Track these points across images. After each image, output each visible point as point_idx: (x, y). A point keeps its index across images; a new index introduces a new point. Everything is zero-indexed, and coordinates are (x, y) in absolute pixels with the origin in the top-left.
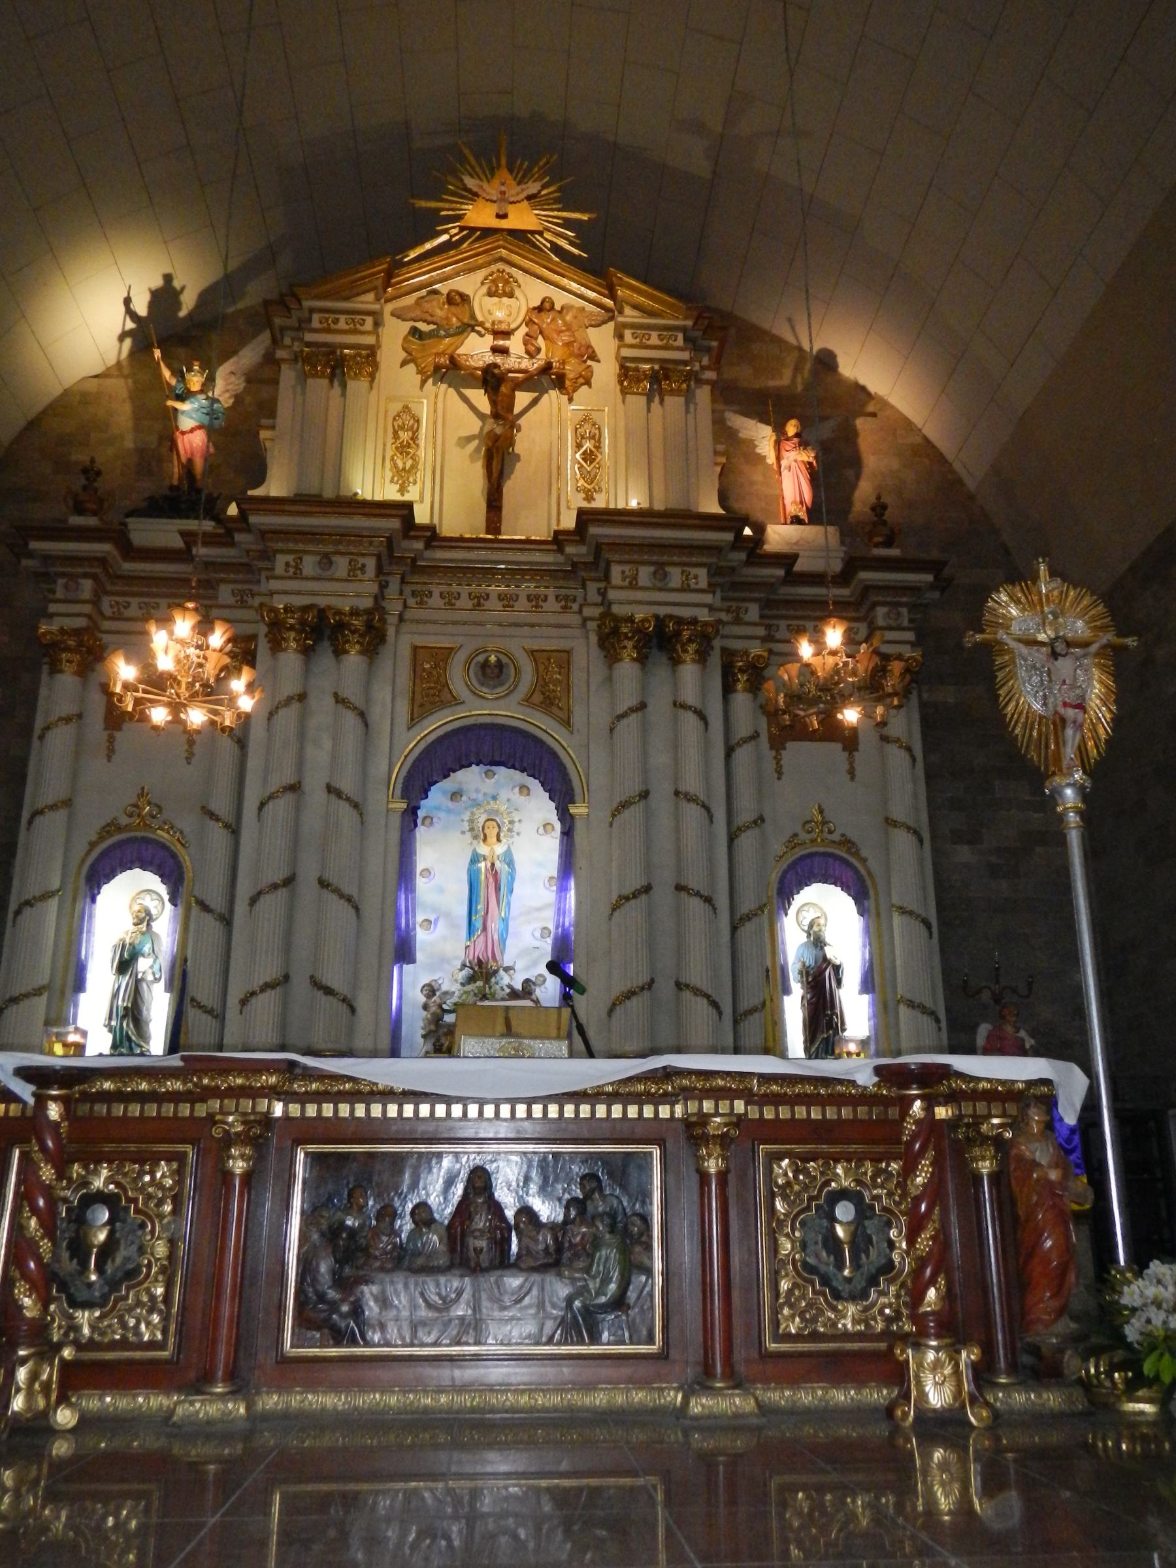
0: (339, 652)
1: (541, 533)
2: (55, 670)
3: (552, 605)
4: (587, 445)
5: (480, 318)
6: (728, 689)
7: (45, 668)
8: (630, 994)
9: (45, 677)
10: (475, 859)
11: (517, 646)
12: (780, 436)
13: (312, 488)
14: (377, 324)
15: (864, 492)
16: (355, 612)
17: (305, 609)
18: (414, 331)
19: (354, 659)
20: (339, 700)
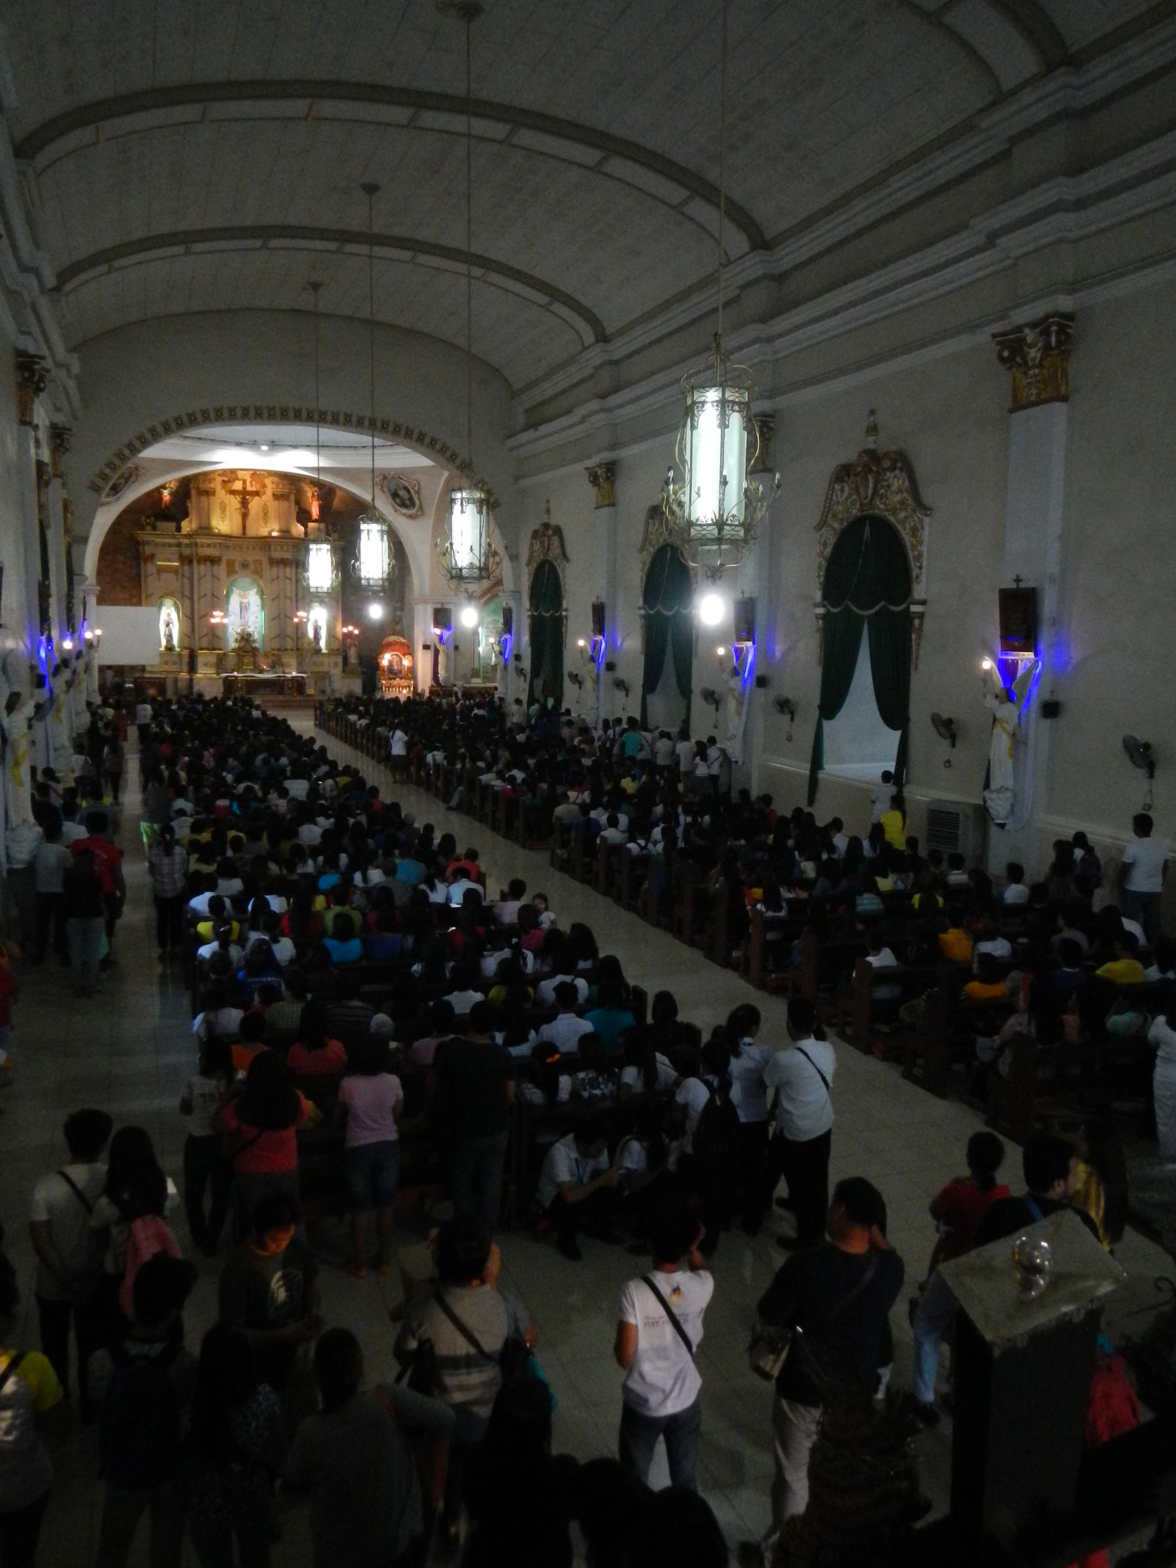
0: (213, 565)
1: (255, 536)
2: (145, 562)
3: (258, 550)
4: (265, 511)
5: (240, 477)
6: (297, 567)
7: (142, 561)
8: (273, 638)
9: (142, 565)
10: (241, 603)
11: (250, 559)
12: (313, 495)
13: (203, 525)
14: (215, 479)
15: (336, 502)
16: (215, 557)
17: (205, 556)
18: (223, 481)
19: (216, 567)
20: (213, 576)
